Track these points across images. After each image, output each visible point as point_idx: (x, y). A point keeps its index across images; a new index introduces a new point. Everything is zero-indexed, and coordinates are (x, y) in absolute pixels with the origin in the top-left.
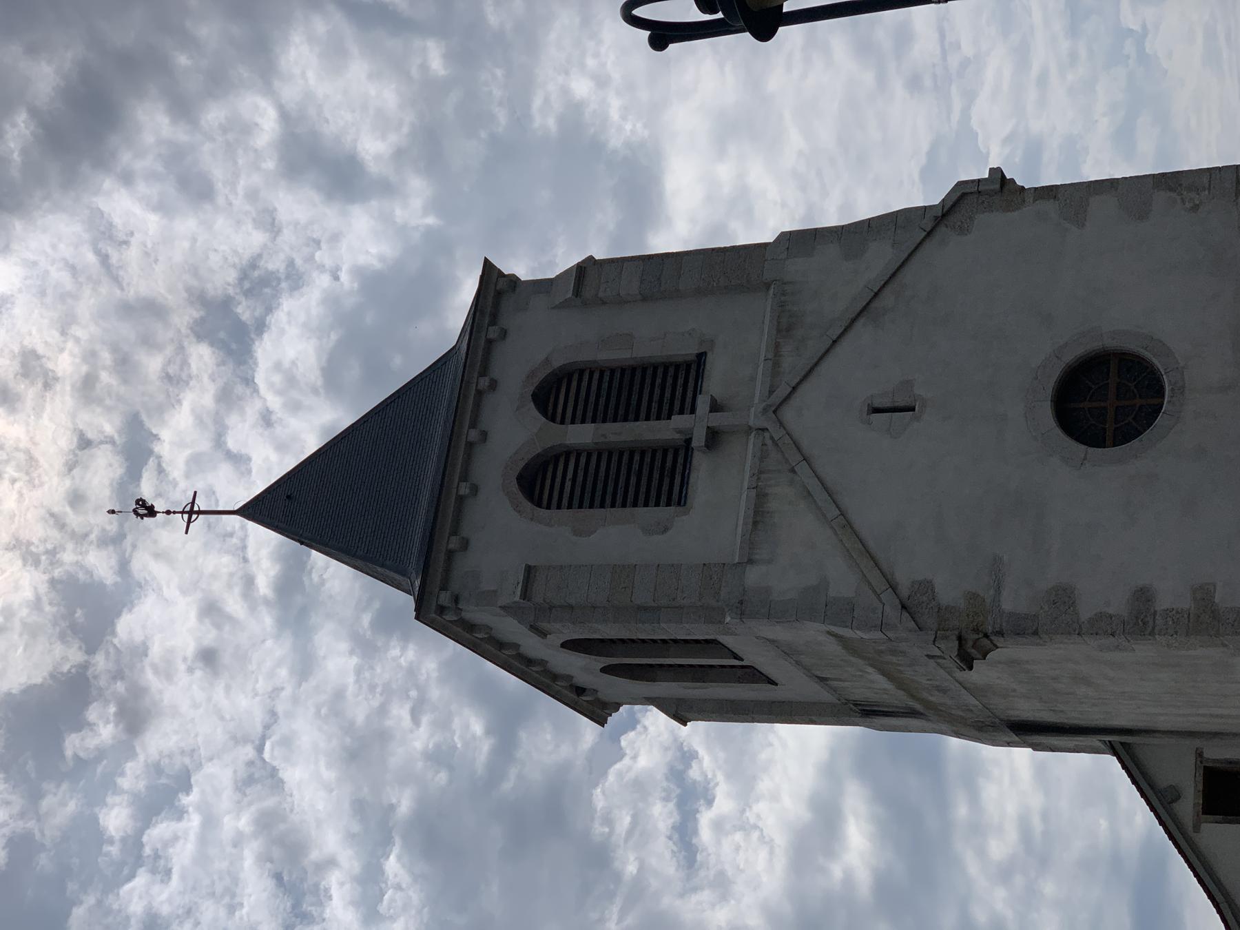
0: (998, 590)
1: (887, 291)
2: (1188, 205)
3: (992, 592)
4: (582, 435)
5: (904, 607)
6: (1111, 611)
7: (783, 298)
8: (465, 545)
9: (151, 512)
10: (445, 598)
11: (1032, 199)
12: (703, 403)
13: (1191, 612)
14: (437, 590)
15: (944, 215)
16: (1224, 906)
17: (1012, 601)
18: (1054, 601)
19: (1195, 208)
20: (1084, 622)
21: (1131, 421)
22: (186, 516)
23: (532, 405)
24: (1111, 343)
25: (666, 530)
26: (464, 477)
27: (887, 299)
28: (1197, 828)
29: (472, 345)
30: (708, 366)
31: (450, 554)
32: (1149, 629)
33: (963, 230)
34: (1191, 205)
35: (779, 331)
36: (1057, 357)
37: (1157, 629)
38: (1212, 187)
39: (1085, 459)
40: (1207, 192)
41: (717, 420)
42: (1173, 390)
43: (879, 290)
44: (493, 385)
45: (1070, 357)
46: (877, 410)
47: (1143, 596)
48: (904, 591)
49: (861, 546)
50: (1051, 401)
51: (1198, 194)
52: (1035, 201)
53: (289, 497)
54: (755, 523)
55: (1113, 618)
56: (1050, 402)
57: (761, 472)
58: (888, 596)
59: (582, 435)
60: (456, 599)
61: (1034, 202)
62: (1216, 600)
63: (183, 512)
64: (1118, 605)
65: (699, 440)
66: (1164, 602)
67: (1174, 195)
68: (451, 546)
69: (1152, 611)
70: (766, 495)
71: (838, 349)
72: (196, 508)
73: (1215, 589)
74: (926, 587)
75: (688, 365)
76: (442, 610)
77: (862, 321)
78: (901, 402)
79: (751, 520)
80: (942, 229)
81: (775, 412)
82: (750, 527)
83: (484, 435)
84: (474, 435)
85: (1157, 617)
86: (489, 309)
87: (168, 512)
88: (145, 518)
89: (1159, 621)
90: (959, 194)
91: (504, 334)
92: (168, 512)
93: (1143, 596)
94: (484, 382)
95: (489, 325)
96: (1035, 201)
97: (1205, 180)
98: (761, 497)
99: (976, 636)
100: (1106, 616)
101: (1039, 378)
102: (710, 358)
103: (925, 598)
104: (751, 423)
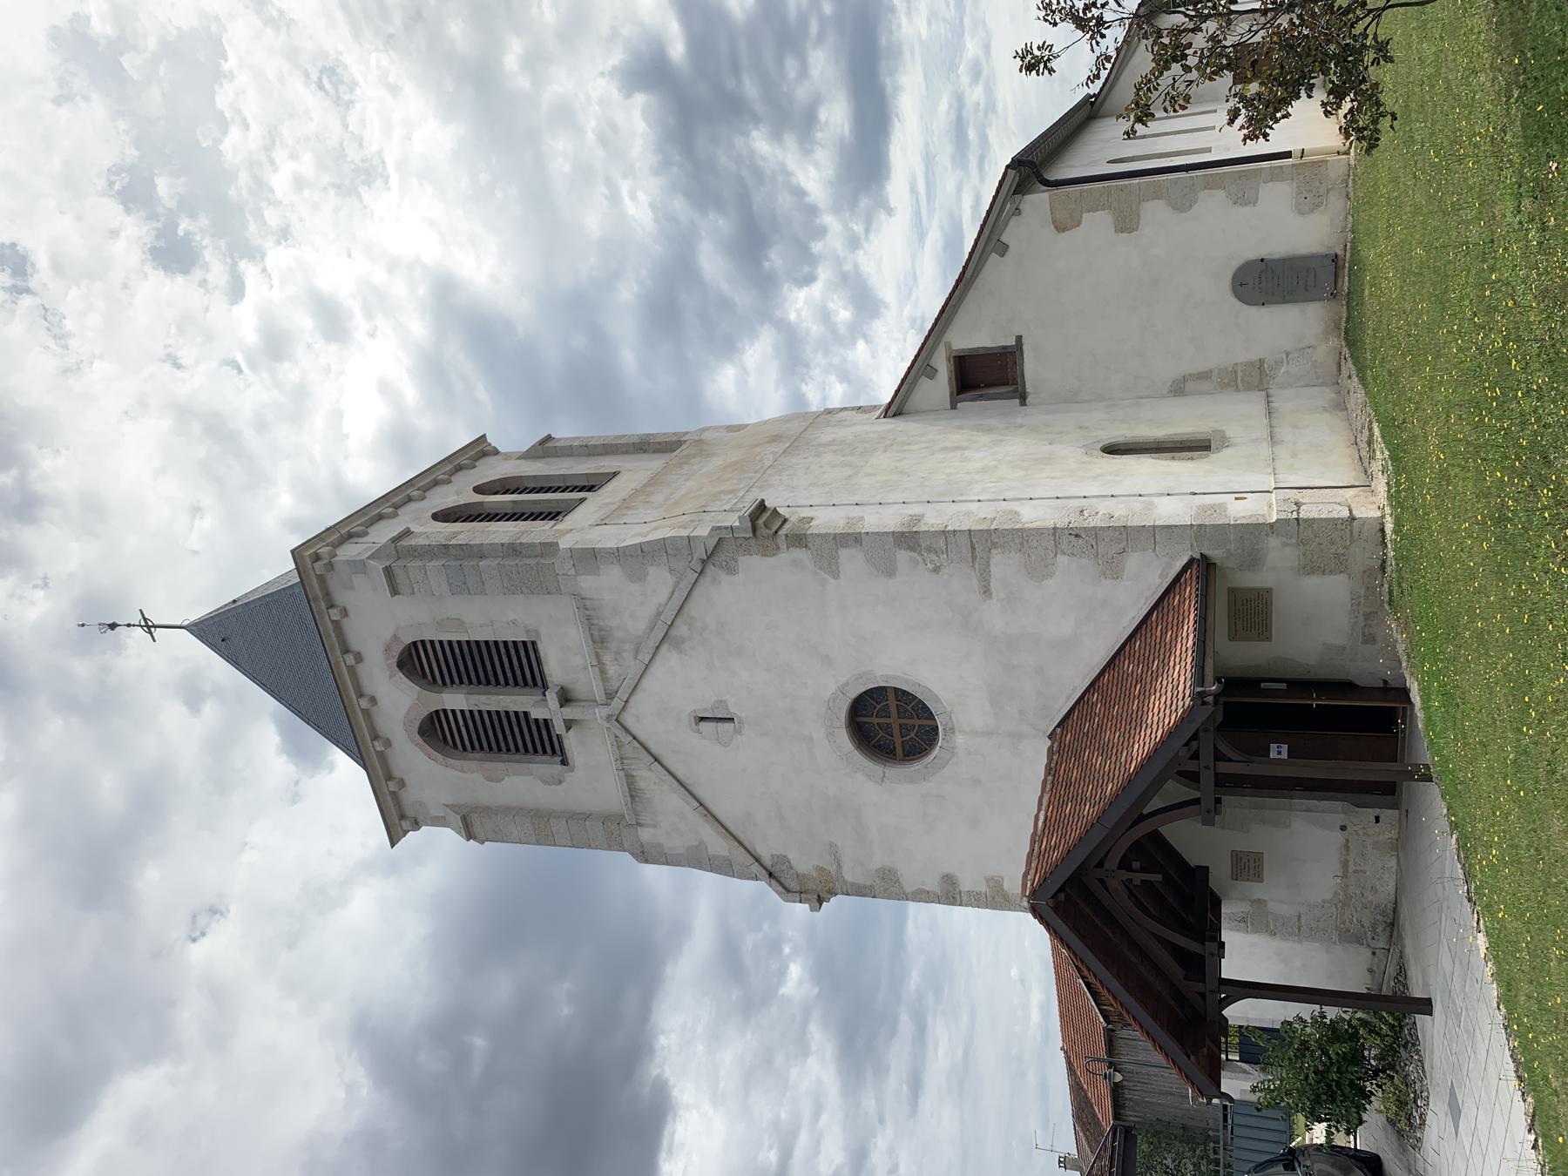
1: (679, 622)
4: (456, 700)
5: (771, 875)
7: (587, 612)
8: (402, 784)
14: (397, 822)
19: (937, 570)
25: (560, 782)
27: (681, 630)
29: (322, 633)
30: (543, 660)
33: (731, 570)
34: (933, 566)
35: (594, 642)
39: (884, 776)
40: (945, 556)
44: (359, 658)
46: (702, 719)
48: (767, 861)
49: (723, 831)
53: (223, 640)
54: (632, 796)
56: (845, 730)
57: (622, 758)
59: (456, 700)
64: (933, 885)
66: (966, 885)
67: (913, 554)
70: (633, 776)
71: (652, 669)
72: (153, 629)
74: (784, 859)
77: (664, 649)
79: (628, 795)
80: (710, 569)
81: (617, 720)
82: (629, 799)
83: (373, 700)
86: (320, 595)
87: (129, 625)
92: (129, 625)
95: (328, 609)
96: (788, 548)
97: (942, 543)
98: (630, 780)
103: (784, 868)
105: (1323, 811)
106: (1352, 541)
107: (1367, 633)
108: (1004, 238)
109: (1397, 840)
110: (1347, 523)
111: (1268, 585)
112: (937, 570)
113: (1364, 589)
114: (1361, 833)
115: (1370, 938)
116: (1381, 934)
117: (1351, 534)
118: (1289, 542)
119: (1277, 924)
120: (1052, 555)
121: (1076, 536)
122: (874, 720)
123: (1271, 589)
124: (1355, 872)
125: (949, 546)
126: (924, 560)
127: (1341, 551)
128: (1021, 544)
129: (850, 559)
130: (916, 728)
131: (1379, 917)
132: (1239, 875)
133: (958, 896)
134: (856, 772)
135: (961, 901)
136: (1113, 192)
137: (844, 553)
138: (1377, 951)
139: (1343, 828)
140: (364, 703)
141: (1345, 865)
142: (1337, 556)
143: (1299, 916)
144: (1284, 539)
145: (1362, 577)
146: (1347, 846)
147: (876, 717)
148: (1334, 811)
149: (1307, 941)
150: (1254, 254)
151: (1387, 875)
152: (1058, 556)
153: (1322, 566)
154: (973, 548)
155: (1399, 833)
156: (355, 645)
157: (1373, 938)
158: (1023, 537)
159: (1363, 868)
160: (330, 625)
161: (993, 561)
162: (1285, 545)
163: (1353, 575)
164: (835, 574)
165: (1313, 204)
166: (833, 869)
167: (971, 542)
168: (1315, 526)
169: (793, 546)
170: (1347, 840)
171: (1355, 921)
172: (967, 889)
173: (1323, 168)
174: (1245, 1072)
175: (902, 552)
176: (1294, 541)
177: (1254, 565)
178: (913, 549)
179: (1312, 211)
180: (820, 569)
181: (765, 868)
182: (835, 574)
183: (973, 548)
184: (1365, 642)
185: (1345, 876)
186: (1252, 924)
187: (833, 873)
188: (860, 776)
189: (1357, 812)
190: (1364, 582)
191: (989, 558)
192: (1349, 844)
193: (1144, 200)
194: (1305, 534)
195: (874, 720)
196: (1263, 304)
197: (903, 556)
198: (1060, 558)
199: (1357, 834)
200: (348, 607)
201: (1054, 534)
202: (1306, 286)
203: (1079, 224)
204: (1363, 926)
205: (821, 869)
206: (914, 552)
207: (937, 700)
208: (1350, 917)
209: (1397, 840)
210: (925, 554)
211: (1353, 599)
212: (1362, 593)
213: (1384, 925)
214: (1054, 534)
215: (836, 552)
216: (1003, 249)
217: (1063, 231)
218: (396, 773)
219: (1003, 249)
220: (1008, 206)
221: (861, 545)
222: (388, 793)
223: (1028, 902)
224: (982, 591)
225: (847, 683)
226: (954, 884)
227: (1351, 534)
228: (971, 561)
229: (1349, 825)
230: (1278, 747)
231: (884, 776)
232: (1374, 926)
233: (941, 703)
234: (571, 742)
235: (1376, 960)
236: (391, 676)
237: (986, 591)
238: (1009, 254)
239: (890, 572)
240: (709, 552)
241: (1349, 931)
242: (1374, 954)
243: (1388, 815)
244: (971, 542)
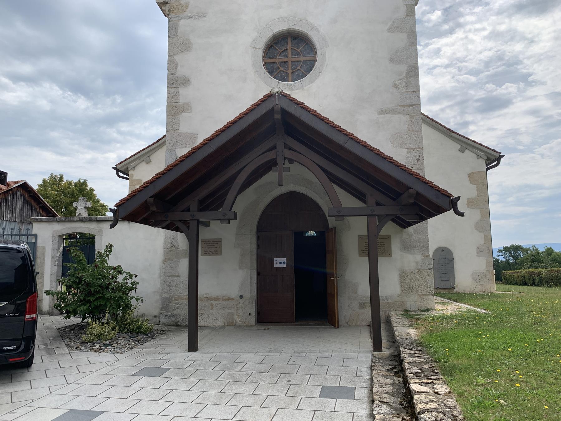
0: (190, 18)
2: (397, 82)
3: (189, 15)
6: (179, 68)
11: (407, 3)
13: (178, 103)
16: (156, 145)
17: (184, 24)
18: (184, 43)
19: (395, 86)
20: (173, 57)
21: (280, 69)
24: (319, 53)
32: (170, 86)
34: (398, 84)
36: (312, 29)
37: (170, 89)
38: (407, 93)
39: (256, 48)
40: (404, 91)
42: (291, 85)
47: (186, 82)
50: (288, 29)
51: (404, 87)
52: (406, 5)
55: (175, 70)
61: (405, 5)
62: (183, 114)
64: (181, 72)
66: (183, 91)
67: (404, 74)
69: (178, 86)
73: (190, 113)
85: (175, 89)
89: (173, 90)
93: (186, 82)
96: (406, 5)
97: (412, 89)
99: (167, 10)
100: (176, 66)
101: (301, 21)
105: (251, 286)
106: (420, 296)
107: (366, 304)
108: (467, 151)
109: (235, 325)
110: (431, 293)
111: (392, 256)
112: (395, 86)
113: (392, 302)
114: (239, 306)
115: (167, 314)
116: (169, 319)
117: (424, 295)
118: (419, 265)
119: (171, 265)
120: (407, 147)
121: (418, 160)
122: (289, 47)
123: (391, 256)
124: (212, 305)
125: (411, 93)
126: (401, 79)
127: (415, 290)
128: (413, 131)
129: (400, 39)
130: (286, 71)
131: (181, 318)
132: (206, 243)
133: (174, 86)
134: (258, 32)
135: (172, 88)
136: (485, 198)
137: (404, 36)
138: (157, 318)
139: (241, 297)
141: (216, 299)
142: (412, 289)
143: (178, 276)
144: (420, 263)
145: (399, 301)
146: (229, 299)
147: (292, 49)
148: (251, 292)
149: (161, 280)
151: (211, 321)
152: (406, 150)
153: (405, 281)
154: (409, 106)
155: (240, 326)
157: (166, 316)
158: (417, 132)
159: (215, 308)
161: (402, 116)
162: (417, 263)
163: (401, 296)
164: (390, 30)
165: (476, 279)
166: (187, 13)
167: (413, 105)
168: (429, 277)
169: (408, 8)
170: (233, 299)
171: (178, 306)
172: (180, 92)
173: (491, 282)
174: (59, 249)
175: (406, 68)
176: (420, 267)
177: (404, 248)
178: (408, 73)
179: (473, 278)
180: (393, 22)
182: (390, 30)
183: (409, 106)
184: (360, 304)
186: (170, 251)
187: (185, 14)
188: (255, 34)
189: (252, 303)
190: (396, 302)
191: (404, 114)
192: (230, 300)
193: (481, 210)
194: (424, 273)
195: (289, 47)
197: (403, 68)
199: (238, 304)
201: (419, 148)
202: (442, 277)
203: (472, 183)
204: (175, 309)
205: (186, 6)
206: (406, 74)
207: (311, 82)
208: (180, 303)
209: (235, 325)
210: (405, 80)
211: (386, 297)
212: (389, 301)
213: (176, 321)
214: (419, 148)
215: (405, 32)
216: (462, 151)
217: (469, 176)
220: (482, 153)
221: (409, 46)
223: (277, 92)
224: (382, 109)
225: (318, 31)
226: (183, 84)
227: (424, 295)
228: (401, 104)
229: (244, 300)
230: (284, 262)
231: (256, 48)
232: (175, 316)
233: (308, 85)
235: (151, 318)
237: (383, 112)
238: (459, 153)
241: (170, 303)
242: (155, 317)
244: (413, 105)
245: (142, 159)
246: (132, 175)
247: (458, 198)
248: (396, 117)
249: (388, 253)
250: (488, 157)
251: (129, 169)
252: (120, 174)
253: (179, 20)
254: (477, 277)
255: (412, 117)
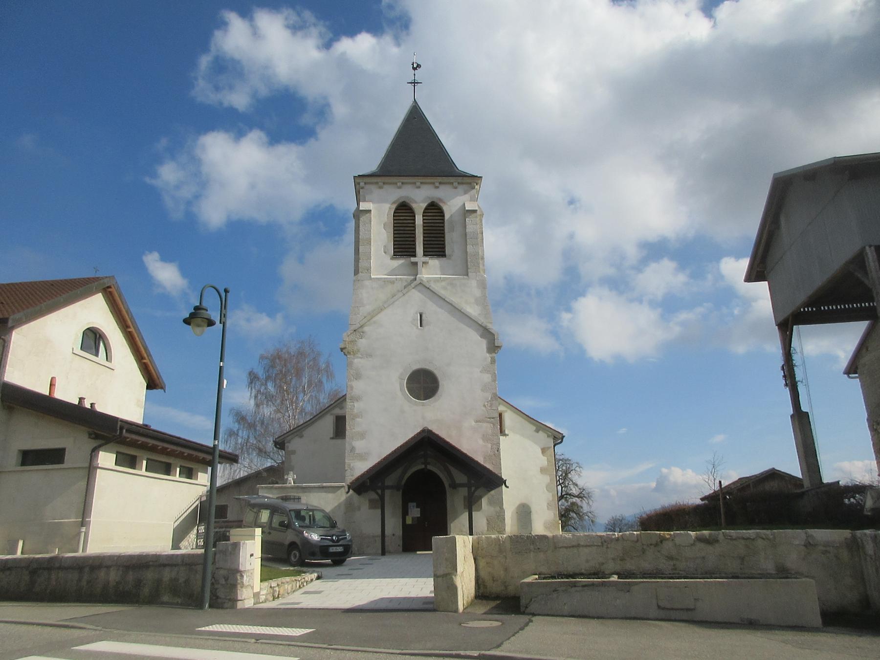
4: (419, 220)
5: (355, 330)
8: (381, 188)
9: (414, 69)
10: (362, 184)
12: (426, 259)
15: (487, 329)
19: (484, 406)
22: (413, 81)
23: (430, 202)
25: (385, 253)
26: (403, 183)
28: (331, 414)
31: (377, 183)
41: (420, 264)
43: (462, 312)
44: (437, 187)
45: (436, 372)
58: (358, 325)
59: (419, 220)
60: (362, 188)
63: (415, 80)
65: (413, 259)
68: (380, 183)
70: (394, 283)
75: (444, 252)
76: (359, 184)
78: (424, 322)
81: (420, 283)
83: (419, 187)
84: (418, 184)
87: (414, 75)
88: (412, 66)
90: (494, 333)
91: (456, 188)
92: (414, 75)
94: (437, 184)
102: (445, 258)
104: (418, 276)
108: (540, 432)
137: (489, 376)
139: (394, 535)
140: (418, 184)
150: (533, 510)
156: (442, 187)
160: (452, 181)
179: (545, 527)
181: (358, 328)
185: (373, 537)
196: (517, 513)
198: (490, 445)
200: (455, 189)
216: (537, 431)
218: (386, 186)
219: (537, 431)
222: (378, 181)
234: (400, 262)
236: (429, 198)
239: (482, 390)
240: (490, 330)
243: (401, 549)
245: (296, 434)
246: (288, 447)
247: (506, 480)
248: (485, 425)
249: (480, 508)
250: (554, 437)
251: (285, 442)
252: (278, 446)
253: (354, 359)
254: (547, 526)
255: (494, 425)
